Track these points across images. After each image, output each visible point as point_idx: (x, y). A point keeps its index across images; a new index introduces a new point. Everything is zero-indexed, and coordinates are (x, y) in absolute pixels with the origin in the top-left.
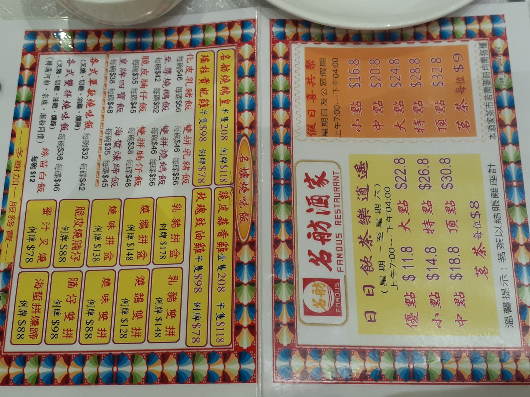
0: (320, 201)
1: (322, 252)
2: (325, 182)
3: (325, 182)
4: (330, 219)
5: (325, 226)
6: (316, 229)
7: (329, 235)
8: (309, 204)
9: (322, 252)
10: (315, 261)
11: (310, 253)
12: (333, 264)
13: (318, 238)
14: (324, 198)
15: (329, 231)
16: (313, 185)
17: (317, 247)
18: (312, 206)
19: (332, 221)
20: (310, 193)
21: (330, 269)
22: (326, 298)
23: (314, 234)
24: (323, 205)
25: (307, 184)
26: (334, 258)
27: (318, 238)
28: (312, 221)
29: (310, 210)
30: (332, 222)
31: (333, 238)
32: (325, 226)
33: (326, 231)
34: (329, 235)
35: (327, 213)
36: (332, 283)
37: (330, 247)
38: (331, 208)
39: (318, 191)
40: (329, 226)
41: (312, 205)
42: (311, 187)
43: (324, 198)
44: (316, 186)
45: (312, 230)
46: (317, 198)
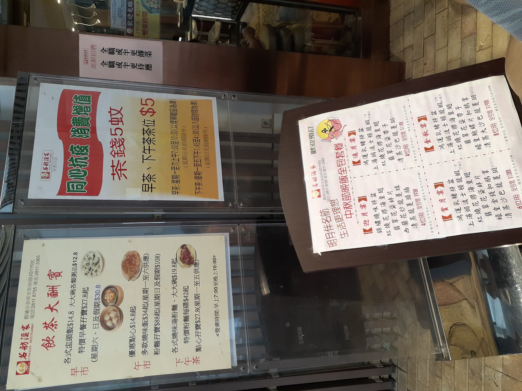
0: (26, 335)
1: (24, 353)
2: (29, 328)
3: (29, 328)
4: (28, 341)
5: (26, 344)
6: (23, 345)
7: (27, 347)
8: (22, 336)
14: (27, 334)
15: (27, 345)
16: (24, 329)
21: (26, 359)
24: (27, 336)
25: (22, 329)
26: (28, 355)
27: (23, 348)
28: (22, 343)
32: (26, 344)
33: (26, 345)
34: (27, 347)
35: (27, 339)
37: (26, 351)
38: (29, 337)
39: (26, 331)
40: (28, 343)
41: (23, 337)
42: (24, 330)
43: (27, 334)
44: (25, 330)
45: (21, 346)
46: (25, 334)
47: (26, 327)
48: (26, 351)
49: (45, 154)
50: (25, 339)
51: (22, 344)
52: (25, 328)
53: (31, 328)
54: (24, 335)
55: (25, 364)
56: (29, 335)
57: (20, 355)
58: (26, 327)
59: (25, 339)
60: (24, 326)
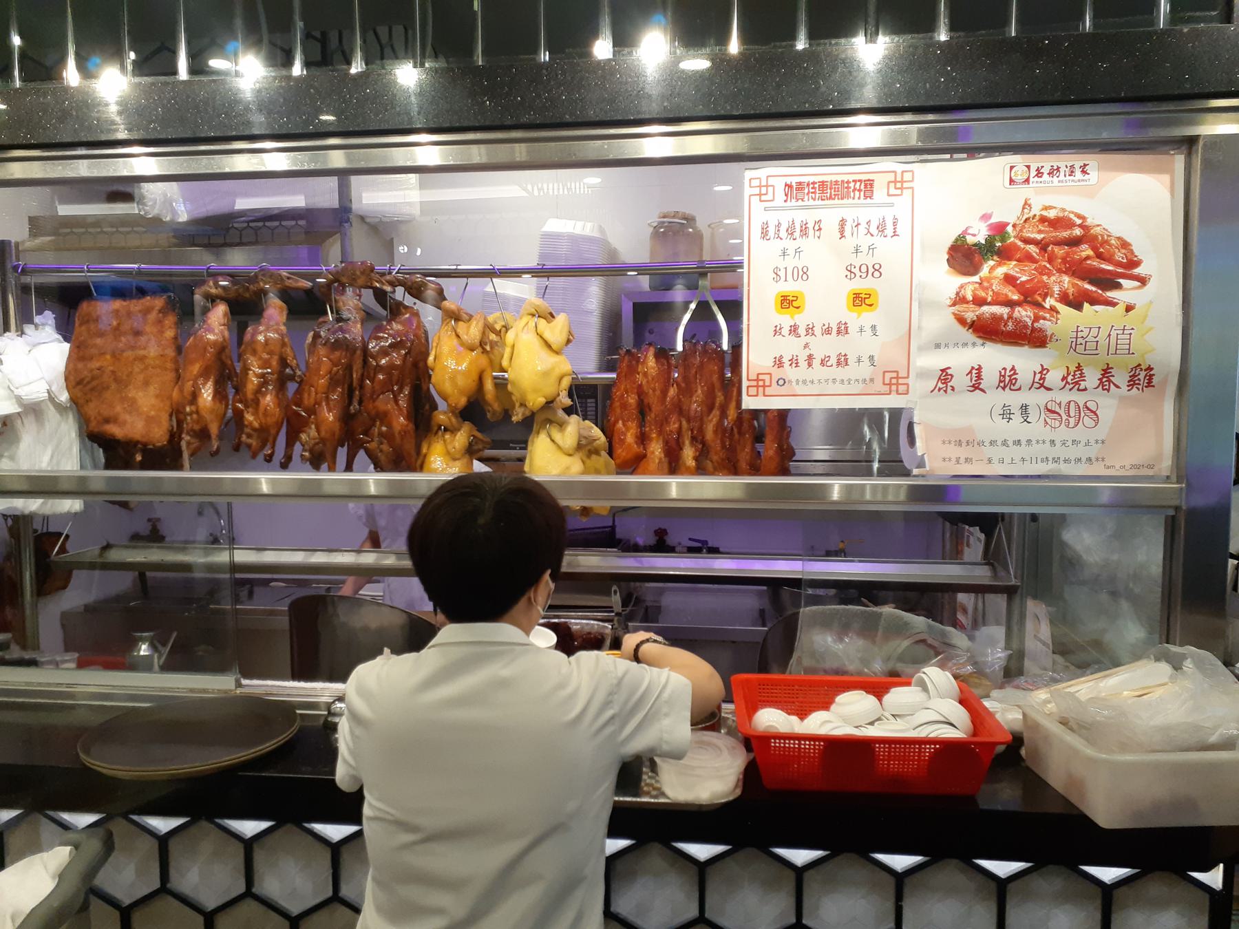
1: (1042, 173)
9: (1042, 173)
10: (1038, 170)
11: (1042, 167)
12: (1036, 178)
15: (1055, 177)
17: (1046, 170)
19: (1060, 178)
20: (1077, 166)
22: (1019, 177)
29: (1067, 167)
30: (1060, 178)
35: (1065, 176)
36: (1027, 181)
37: (1046, 177)
38: (1068, 178)
45: (1055, 168)
48: (1046, 177)
49: (1085, 165)
53: (1084, 178)
60: (1087, 167)
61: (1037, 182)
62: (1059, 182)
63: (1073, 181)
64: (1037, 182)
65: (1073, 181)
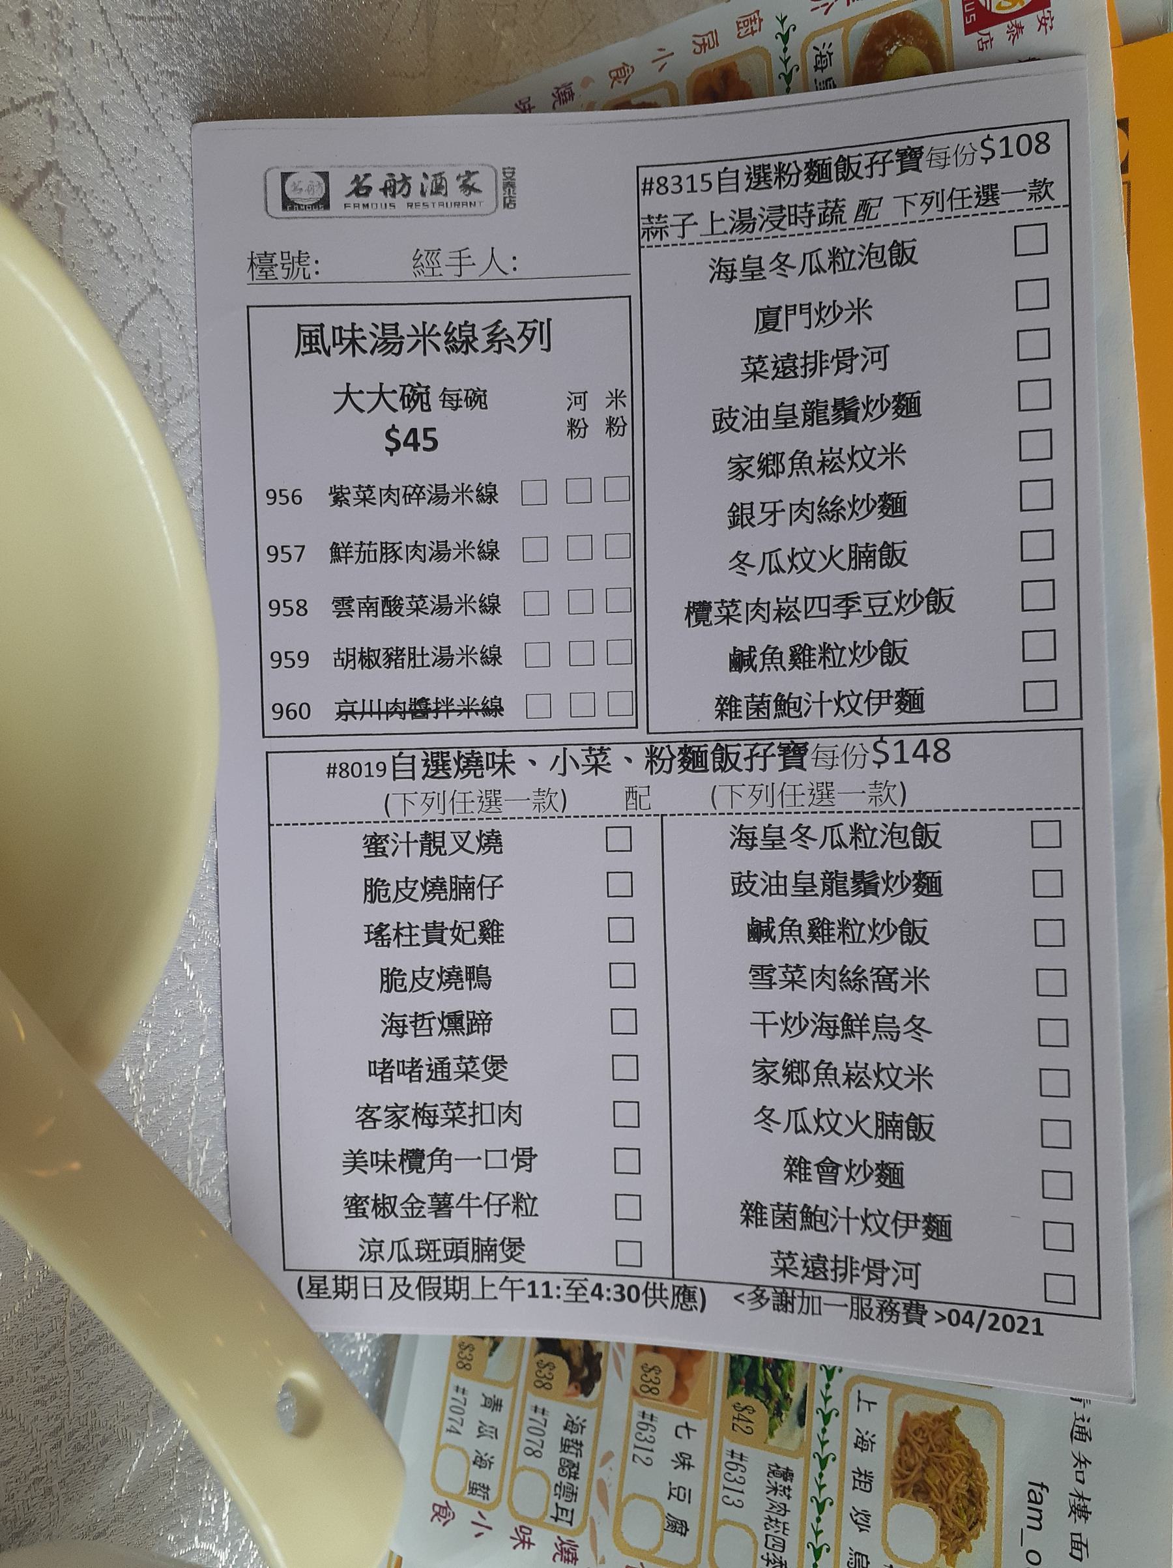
1: (369, 188)
4: (415, 196)
5: (405, 191)
6: (399, 182)
9: (369, 188)
13: (388, 185)
15: (399, 196)
18: (431, 178)
23: (394, 180)
30: (409, 199)
31: (389, 199)
32: (405, 191)
34: (393, 195)
35: (423, 193)
37: (376, 196)
38: (429, 198)
45: (398, 177)
47: (470, 183)
48: (376, 196)
50: (422, 185)
51: (405, 179)
52: (465, 181)
54: (439, 182)
55: (319, 194)
56: (440, 198)
57: (362, 178)
58: (470, 183)
59: (422, 185)
61: (356, 206)
62: (410, 205)
63: (441, 204)
64: (356, 206)
65: (441, 204)
